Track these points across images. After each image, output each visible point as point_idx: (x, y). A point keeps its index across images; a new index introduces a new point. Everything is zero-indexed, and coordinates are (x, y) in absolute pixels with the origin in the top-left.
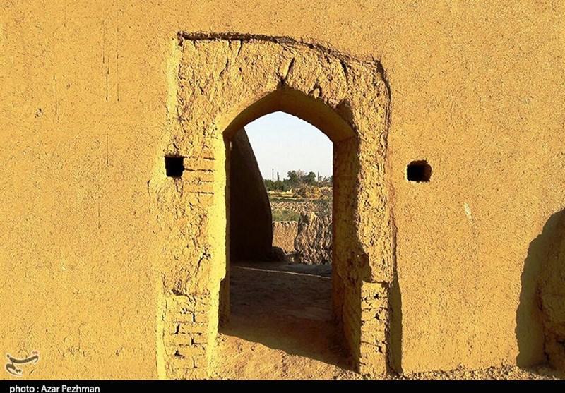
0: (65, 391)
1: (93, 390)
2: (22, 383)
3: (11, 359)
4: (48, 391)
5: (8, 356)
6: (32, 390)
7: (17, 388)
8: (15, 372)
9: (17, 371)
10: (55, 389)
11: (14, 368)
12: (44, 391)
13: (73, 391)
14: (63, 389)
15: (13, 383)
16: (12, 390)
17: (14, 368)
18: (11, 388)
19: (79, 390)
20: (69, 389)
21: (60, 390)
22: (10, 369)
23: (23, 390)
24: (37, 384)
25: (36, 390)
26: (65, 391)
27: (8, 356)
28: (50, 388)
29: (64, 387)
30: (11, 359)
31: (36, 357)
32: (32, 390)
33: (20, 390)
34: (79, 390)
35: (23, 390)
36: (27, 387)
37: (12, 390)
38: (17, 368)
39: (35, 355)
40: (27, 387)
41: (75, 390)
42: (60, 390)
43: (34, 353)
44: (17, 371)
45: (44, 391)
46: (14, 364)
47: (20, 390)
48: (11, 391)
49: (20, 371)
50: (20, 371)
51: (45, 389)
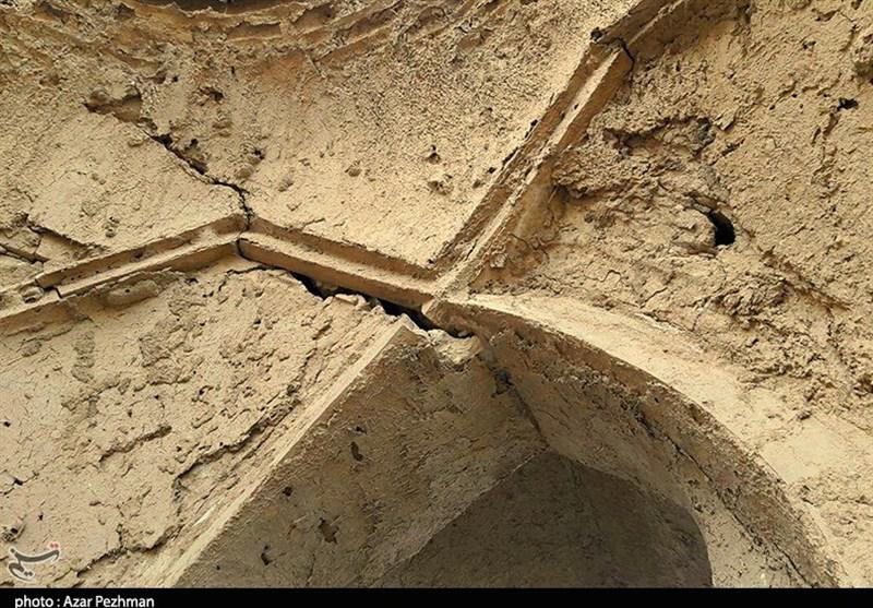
0: (101, 604)
1: (143, 603)
2: (33, 593)
3: (17, 555)
4: (75, 605)
5: (13, 551)
6: (49, 603)
7: (26, 600)
8: (24, 577)
9: (26, 574)
10: (85, 602)
11: (21, 569)
12: (68, 605)
13: (113, 605)
14: (98, 602)
15: (21, 592)
16: (19, 603)
17: (21, 569)
18: (17, 601)
19: (122, 603)
20: (106, 602)
21: (93, 603)
22: (15, 571)
23: (36, 603)
24: (57, 594)
25: (56, 603)
26: (101, 604)
27: (13, 551)
28: (78, 600)
29: (99, 599)
30: (17, 555)
31: (57, 553)
32: (49, 603)
33: (32, 603)
34: (122, 603)
35: (36, 603)
36: (42, 599)
37: (19, 603)
38: (26, 570)
39: (54, 549)
40: (42, 599)
41: (117, 603)
42: (93, 603)
43: (52, 546)
44: (26, 574)
45: (68, 605)
46: (22, 563)
47: (32, 603)
48: (17, 605)
49: (31, 574)
50: (31, 574)
51: (70, 603)
